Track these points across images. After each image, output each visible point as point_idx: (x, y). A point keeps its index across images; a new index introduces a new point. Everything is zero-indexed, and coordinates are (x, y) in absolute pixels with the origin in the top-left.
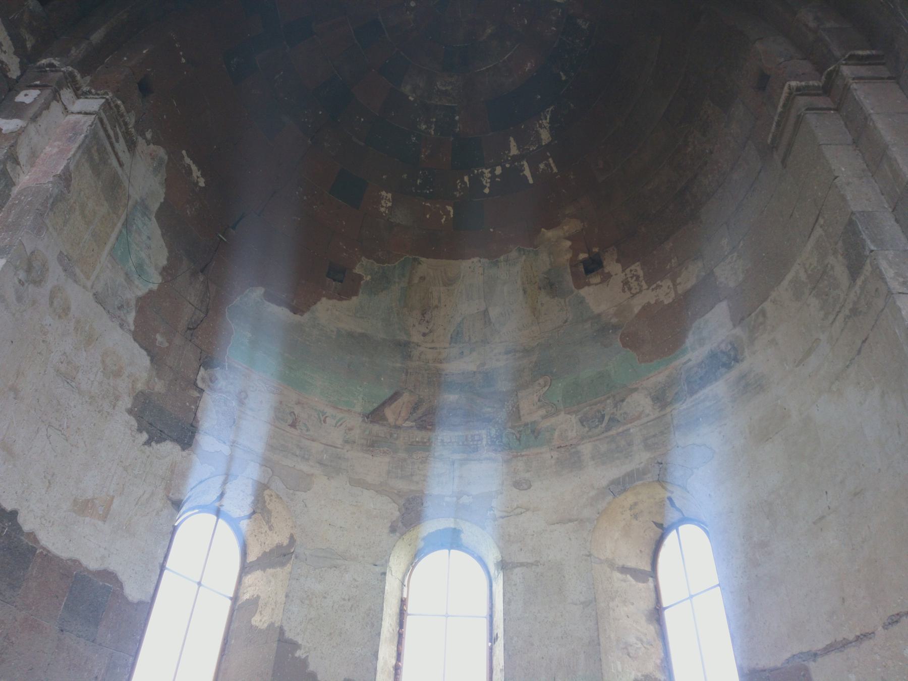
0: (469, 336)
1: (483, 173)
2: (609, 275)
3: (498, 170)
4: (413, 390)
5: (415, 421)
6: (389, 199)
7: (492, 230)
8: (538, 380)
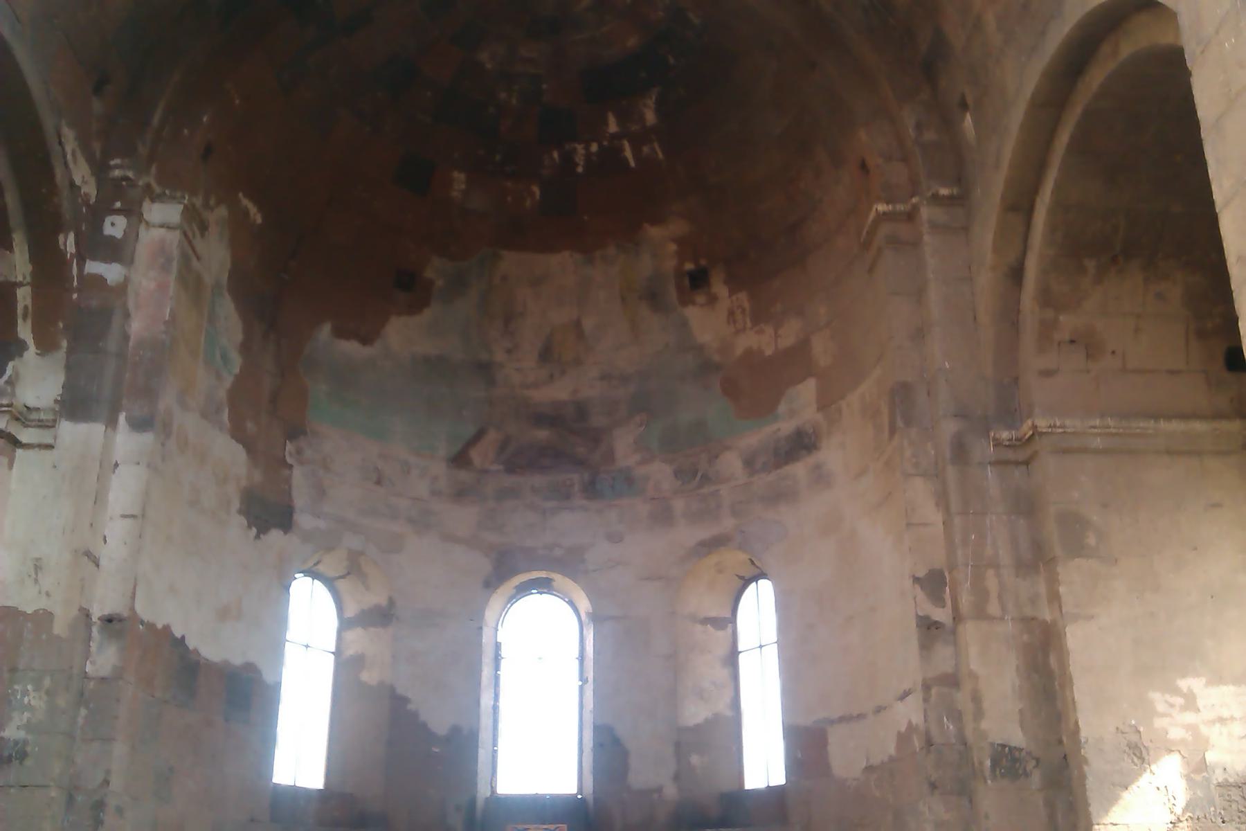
1: (575, 149)
3: (594, 147)
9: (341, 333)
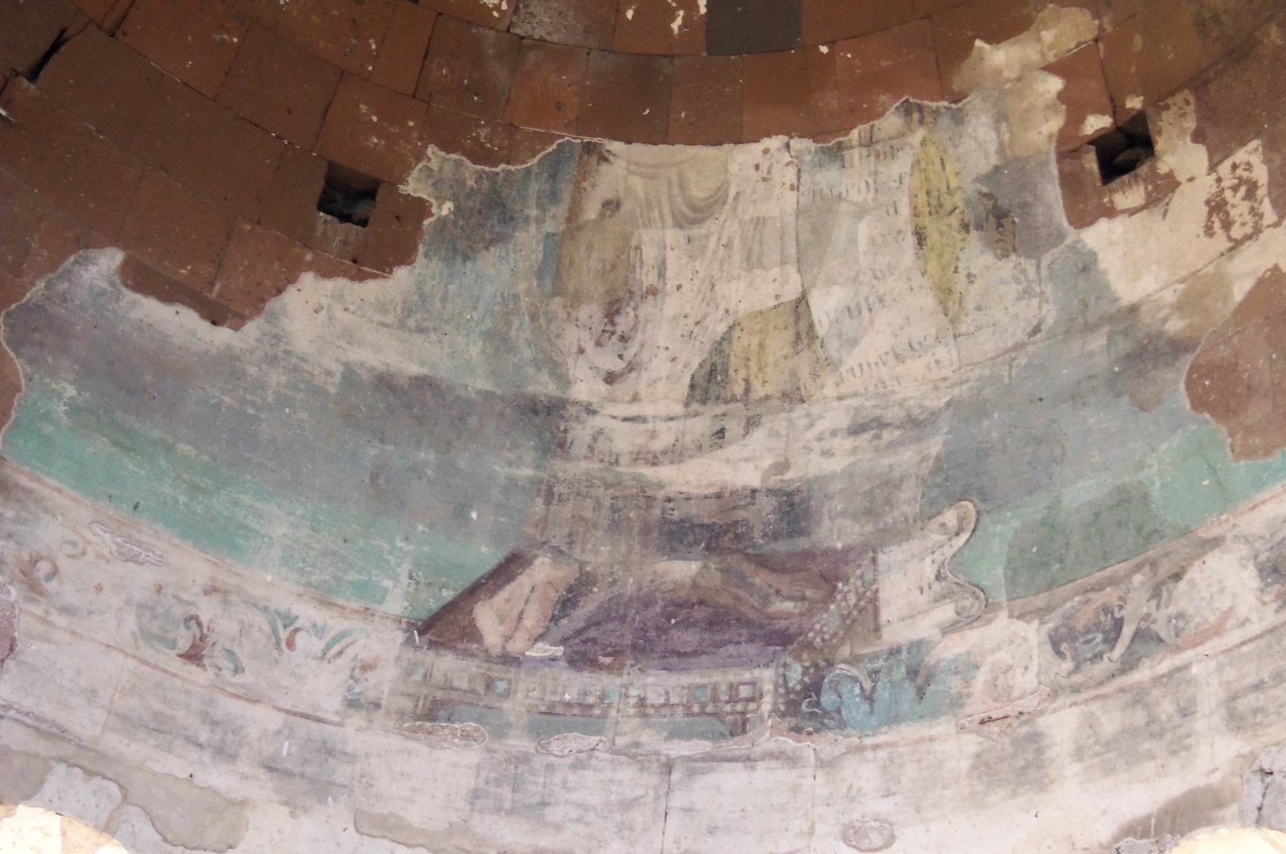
0: (746, 380)
2: (1169, 184)
4: (564, 548)
5: (564, 641)
7: (824, 49)
8: (939, 513)
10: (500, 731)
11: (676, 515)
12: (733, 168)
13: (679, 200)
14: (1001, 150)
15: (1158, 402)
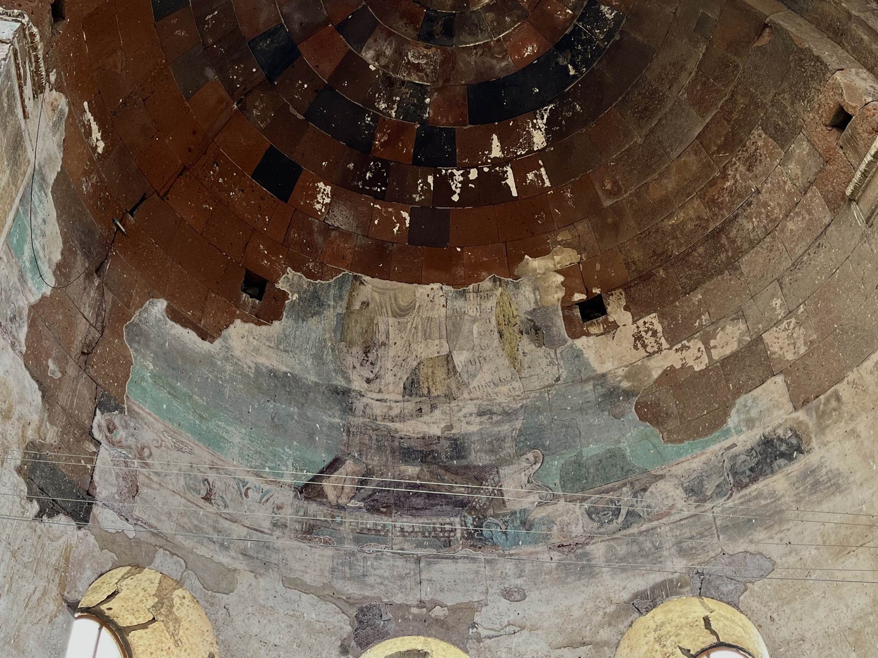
1: (452, 175)
2: (615, 326)
3: (473, 174)
5: (364, 500)
6: (328, 194)
7: (459, 249)
9: (174, 315)
10: (341, 541)
11: (406, 445)
12: (418, 294)
13: (394, 305)
14: (536, 302)
15: (623, 416)
